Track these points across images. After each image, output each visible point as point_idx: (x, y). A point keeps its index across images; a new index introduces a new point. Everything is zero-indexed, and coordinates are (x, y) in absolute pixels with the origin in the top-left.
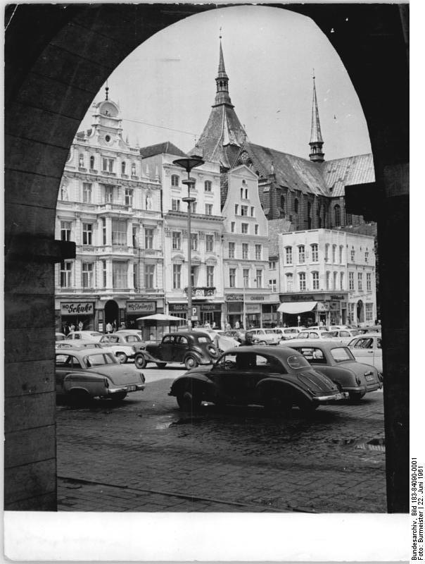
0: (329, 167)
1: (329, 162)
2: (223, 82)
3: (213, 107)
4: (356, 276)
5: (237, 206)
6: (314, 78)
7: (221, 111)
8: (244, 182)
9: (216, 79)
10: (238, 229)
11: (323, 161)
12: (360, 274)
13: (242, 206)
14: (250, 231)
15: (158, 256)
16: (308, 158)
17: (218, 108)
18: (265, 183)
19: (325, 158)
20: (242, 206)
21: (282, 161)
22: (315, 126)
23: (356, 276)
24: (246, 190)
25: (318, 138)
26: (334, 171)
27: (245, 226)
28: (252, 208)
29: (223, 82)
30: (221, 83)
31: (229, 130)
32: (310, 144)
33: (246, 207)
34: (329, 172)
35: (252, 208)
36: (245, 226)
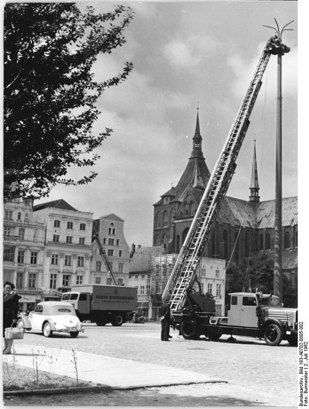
0: (261, 207)
1: (262, 202)
2: (198, 139)
3: (189, 159)
6: (255, 141)
9: (193, 139)
11: (259, 201)
16: (248, 200)
19: (261, 200)
20: (109, 239)
22: (254, 176)
25: (255, 185)
26: (264, 209)
28: (118, 241)
29: (198, 139)
30: (196, 141)
33: (113, 240)
34: (260, 210)
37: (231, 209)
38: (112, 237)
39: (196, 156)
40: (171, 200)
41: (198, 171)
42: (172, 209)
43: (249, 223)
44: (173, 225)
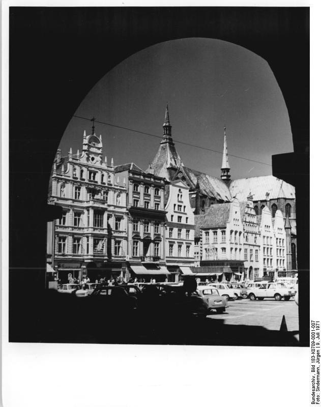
4: (248, 251)
5: (175, 205)
7: (166, 146)
8: (180, 190)
10: (175, 220)
13: (179, 206)
14: (183, 221)
15: (124, 235)
17: (164, 144)
18: (192, 192)
20: (179, 206)
21: (204, 178)
23: (248, 251)
24: (181, 195)
27: (180, 218)
28: (185, 207)
30: (167, 129)
31: (171, 158)
34: (233, 187)
35: (185, 207)
36: (180, 218)
38: (180, 204)
39: (168, 141)
43: (226, 197)
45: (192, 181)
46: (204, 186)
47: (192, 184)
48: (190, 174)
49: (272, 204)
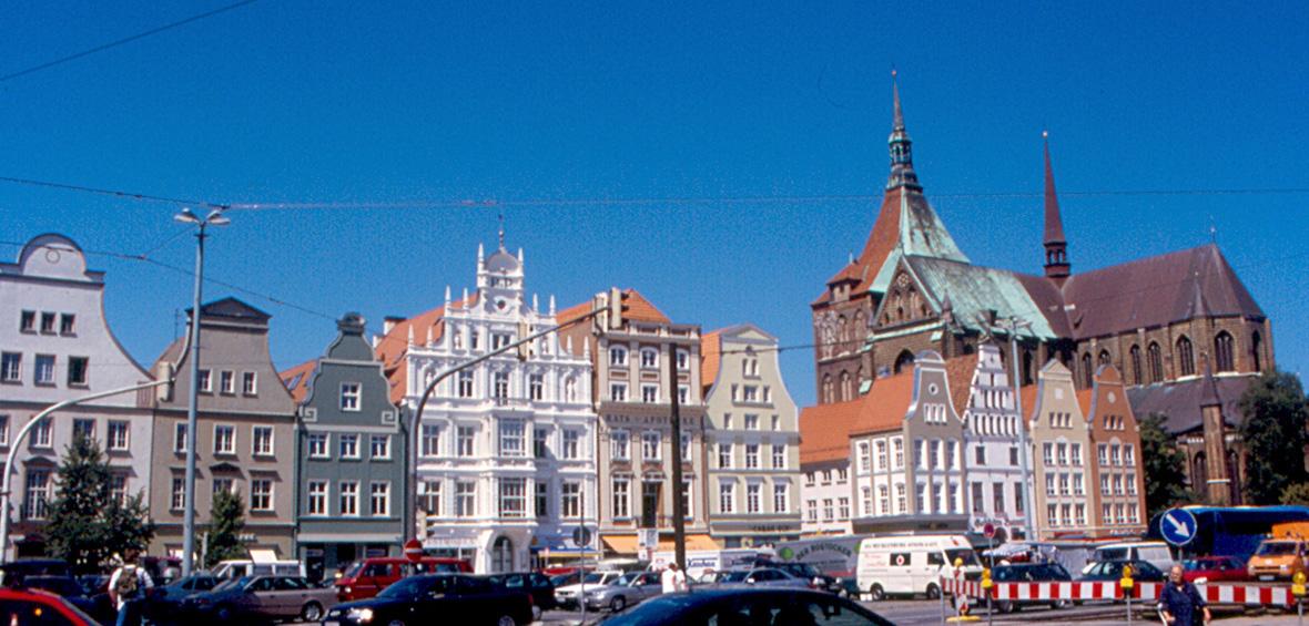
5: (734, 389)
12: (998, 487)
18: (934, 325)
28: (766, 390)
32: (1046, 245)
35: (766, 390)
37: (1007, 297)
40: (853, 287)
41: (909, 216)
42: (859, 310)
44: (868, 347)
45: (932, 294)
46: (973, 302)
47: (932, 301)
48: (931, 273)
49: (1175, 338)
